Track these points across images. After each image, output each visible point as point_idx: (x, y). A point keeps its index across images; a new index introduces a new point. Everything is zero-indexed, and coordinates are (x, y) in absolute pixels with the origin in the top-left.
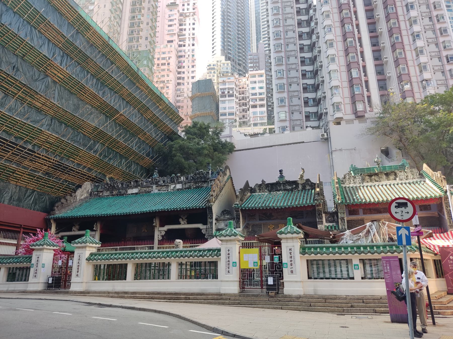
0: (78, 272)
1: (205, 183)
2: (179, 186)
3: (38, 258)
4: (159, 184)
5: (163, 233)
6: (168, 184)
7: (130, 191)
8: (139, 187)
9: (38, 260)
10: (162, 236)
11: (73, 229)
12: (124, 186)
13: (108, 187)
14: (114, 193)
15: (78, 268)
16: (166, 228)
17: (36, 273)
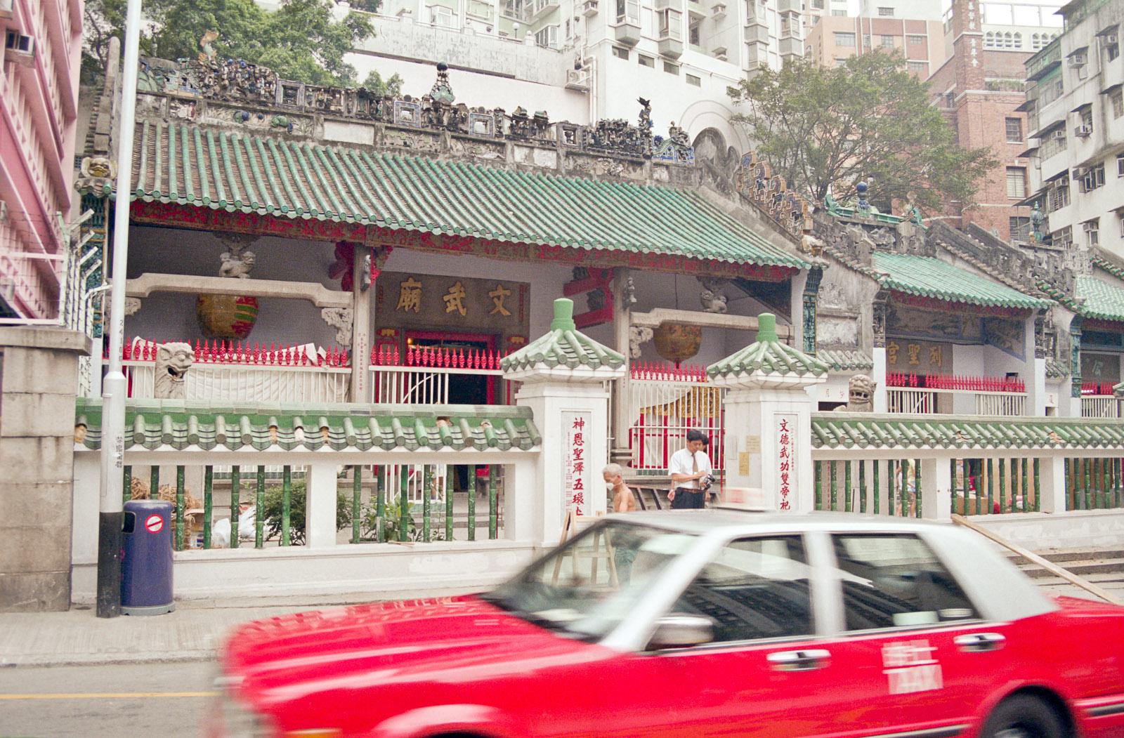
0: (785, 491)
1: (635, 170)
2: (545, 159)
3: (579, 424)
4: (466, 132)
5: (648, 335)
6: (503, 140)
7: (333, 131)
8: (377, 124)
9: (578, 436)
10: (642, 346)
11: (226, 266)
12: (301, 101)
13: (217, 88)
14: (254, 122)
15: (785, 477)
16: (656, 317)
17: (578, 499)
